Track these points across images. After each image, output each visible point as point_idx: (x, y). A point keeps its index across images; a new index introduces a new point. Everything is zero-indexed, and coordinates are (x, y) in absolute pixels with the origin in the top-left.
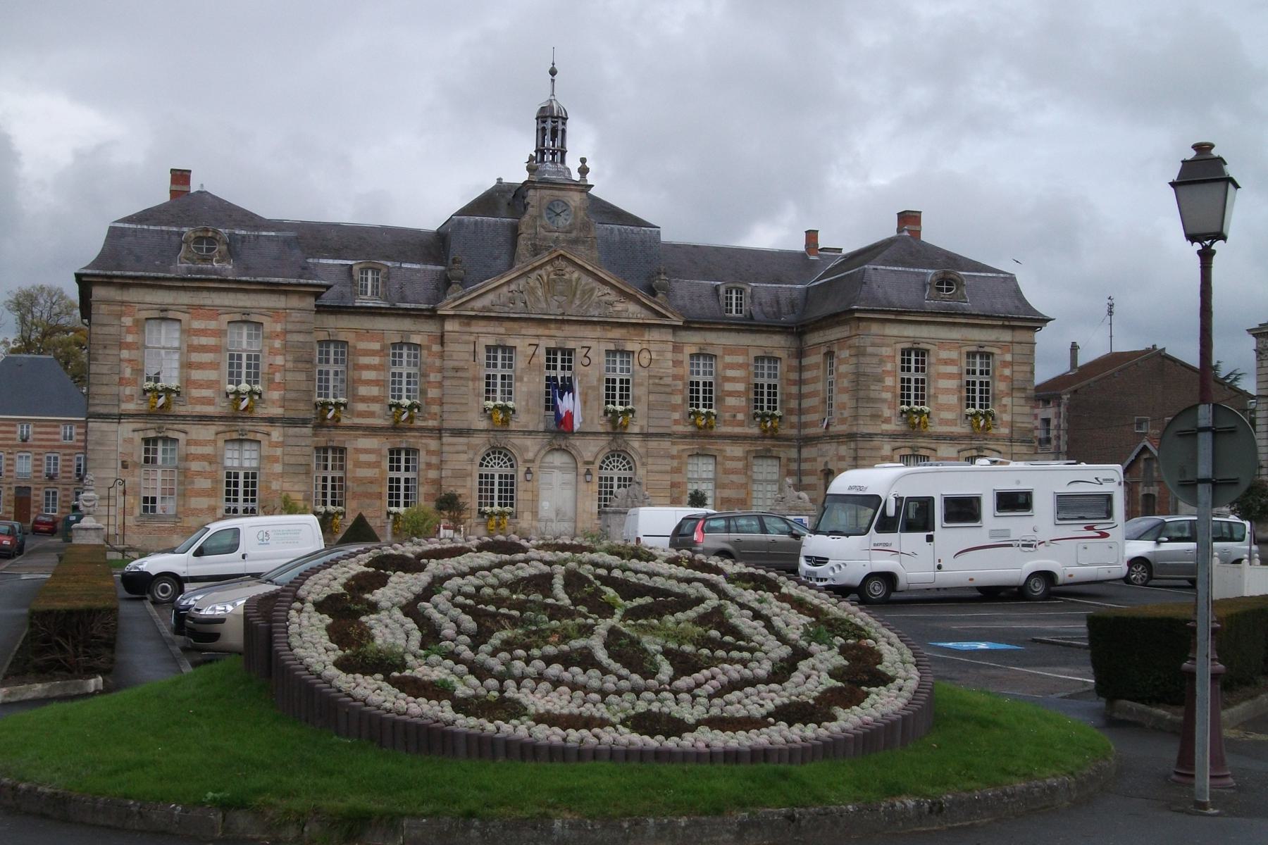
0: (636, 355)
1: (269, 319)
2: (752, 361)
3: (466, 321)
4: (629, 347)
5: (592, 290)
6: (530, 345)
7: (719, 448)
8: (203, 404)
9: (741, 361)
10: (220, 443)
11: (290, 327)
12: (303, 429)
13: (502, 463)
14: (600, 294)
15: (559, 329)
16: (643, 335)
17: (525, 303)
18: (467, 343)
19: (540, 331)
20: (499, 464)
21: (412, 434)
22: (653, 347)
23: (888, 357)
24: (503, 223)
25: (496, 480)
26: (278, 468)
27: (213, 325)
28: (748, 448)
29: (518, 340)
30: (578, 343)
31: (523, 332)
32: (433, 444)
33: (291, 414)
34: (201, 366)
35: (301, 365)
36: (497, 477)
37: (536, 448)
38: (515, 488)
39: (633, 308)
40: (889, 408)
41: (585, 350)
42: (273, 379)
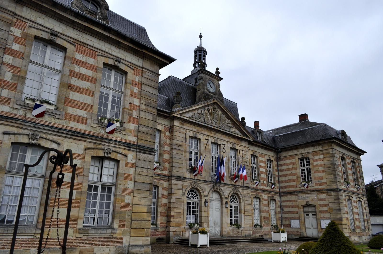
0: (239, 151)
1: (132, 71)
2: (266, 161)
3: (182, 122)
4: (237, 147)
5: (225, 120)
6: (206, 139)
7: (261, 195)
8: (77, 121)
9: (263, 160)
10: (88, 158)
11: (144, 81)
12: (149, 156)
14: (227, 123)
15: (215, 134)
16: (240, 143)
17: (204, 120)
18: (182, 133)
20: (193, 197)
21: (156, 177)
22: (244, 149)
26: (130, 185)
27: (91, 61)
28: (268, 196)
29: (201, 136)
30: (221, 142)
31: (203, 132)
33: (141, 143)
34: (79, 90)
35: (150, 109)
37: (209, 190)
39: (237, 131)
41: (224, 146)
42: (131, 114)
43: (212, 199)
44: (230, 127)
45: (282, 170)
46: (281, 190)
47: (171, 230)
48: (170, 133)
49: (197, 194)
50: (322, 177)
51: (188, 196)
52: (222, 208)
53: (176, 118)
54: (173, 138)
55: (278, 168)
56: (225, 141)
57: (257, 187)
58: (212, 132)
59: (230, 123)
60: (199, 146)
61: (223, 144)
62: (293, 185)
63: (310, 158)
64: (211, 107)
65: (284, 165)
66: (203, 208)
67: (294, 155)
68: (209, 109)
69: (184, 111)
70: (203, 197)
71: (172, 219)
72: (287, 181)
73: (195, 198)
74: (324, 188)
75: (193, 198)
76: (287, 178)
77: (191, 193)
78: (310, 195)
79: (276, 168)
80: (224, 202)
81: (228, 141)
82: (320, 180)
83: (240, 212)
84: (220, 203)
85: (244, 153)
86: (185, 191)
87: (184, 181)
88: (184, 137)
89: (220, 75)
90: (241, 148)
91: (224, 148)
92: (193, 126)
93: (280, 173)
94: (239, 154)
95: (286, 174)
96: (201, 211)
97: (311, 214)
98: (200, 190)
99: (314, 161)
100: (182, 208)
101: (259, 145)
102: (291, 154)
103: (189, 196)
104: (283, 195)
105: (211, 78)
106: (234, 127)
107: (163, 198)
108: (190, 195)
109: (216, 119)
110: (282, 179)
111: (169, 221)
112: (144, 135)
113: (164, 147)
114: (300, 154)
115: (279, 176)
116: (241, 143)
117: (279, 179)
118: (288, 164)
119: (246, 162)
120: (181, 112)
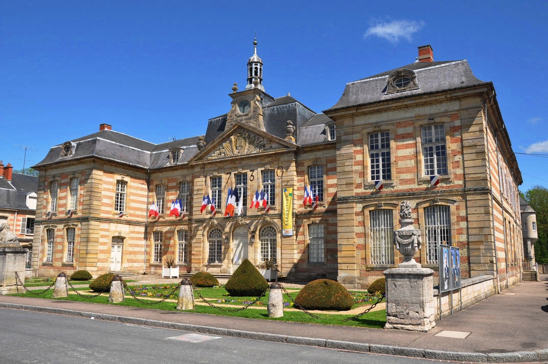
13: (218, 235)
14: (258, 142)
15: (240, 163)
16: (279, 160)
20: (217, 235)
23: (358, 140)
25: (216, 244)
35: (88, 193)
40: (360, 177)
71: (193, 257)
77: (215, 232)
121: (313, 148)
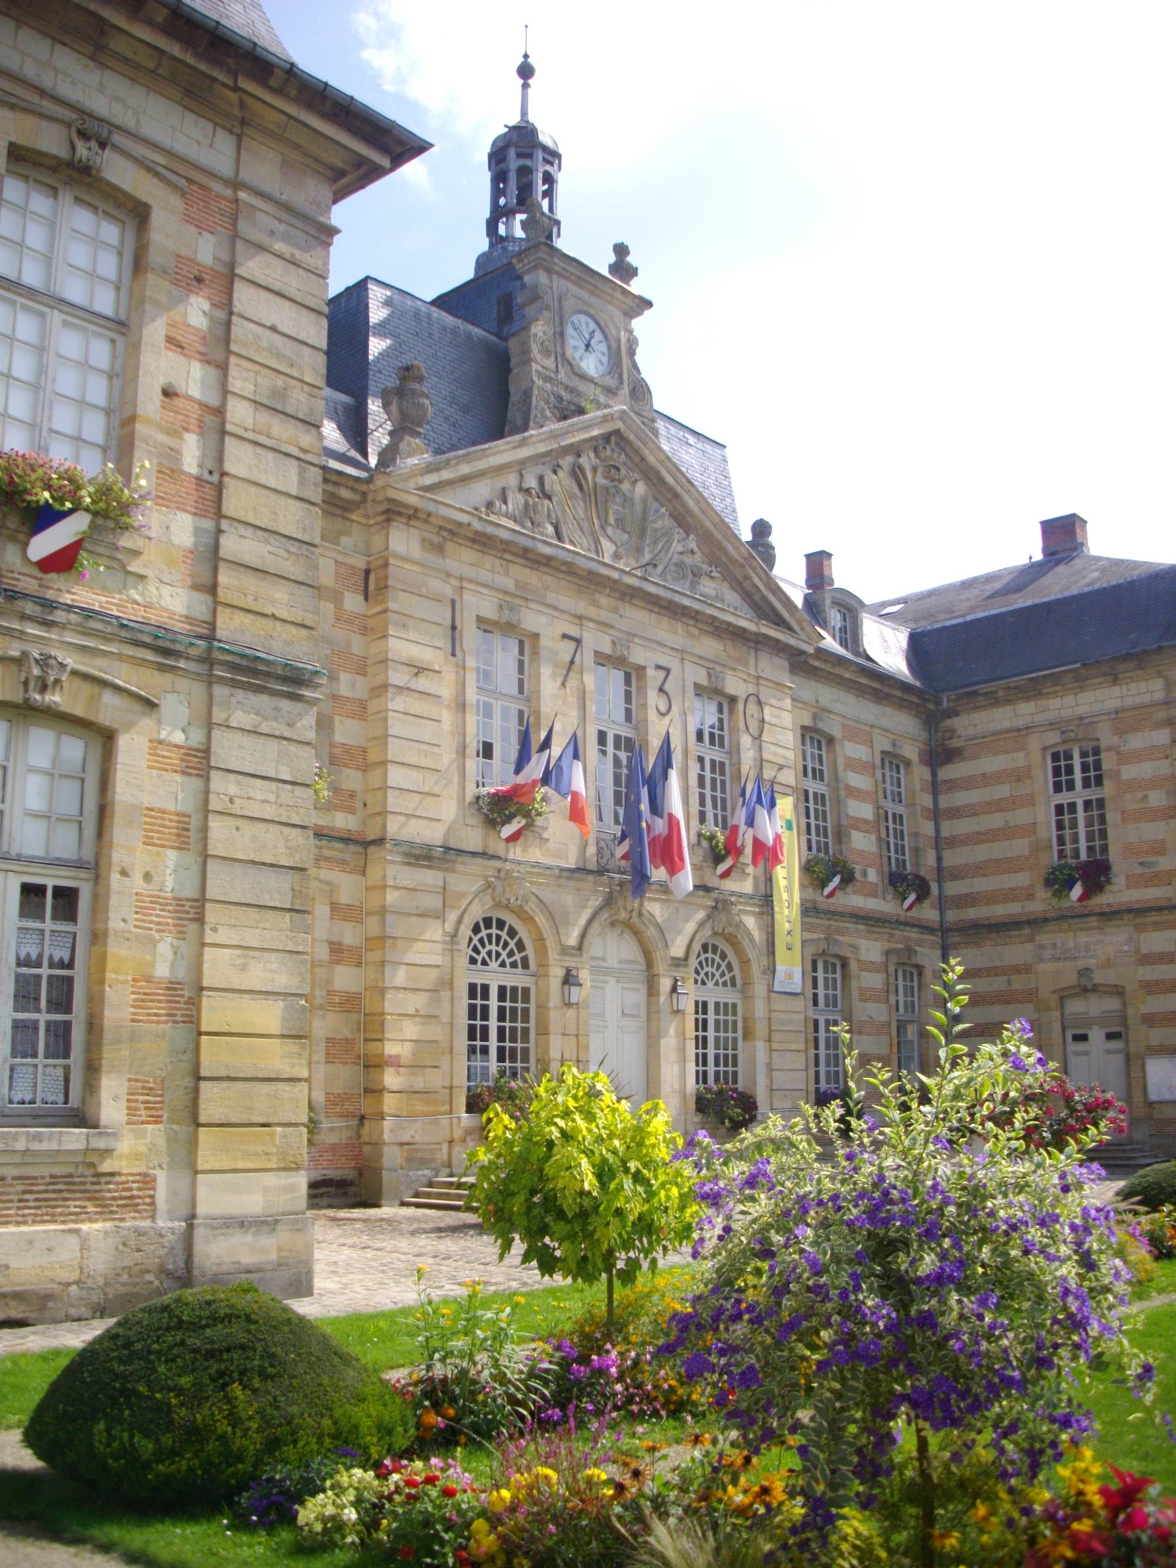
0: (740, 706)
1: (175, 201)
5: (668, 533)
6: (565, 636)
9: (864, 758)
13: (504, 954)
14: (680, 549)
15: (615, 610)
16: (746, 664)
19: (582, 606)
20: (498, 955)
24: (469, 336)
28: (887, 945)
29: (543, 620)
30: (649, 654)
31: (551, 597)
32: (348, 887)
36: (494, 993)
38: (532, 1024)
41: (662, 674)
43: (603, 964)
44: (696, 574)
45: (955, 813)
46: (952, 916)
47: (387, 1137)
48: (366, 599)
49: (520, 941)
50: (1163, 841)
51: (476, 950)
52: (652, 1011)
53: (399, 513)
54: (386, 629)
55: (935, 802)
56: (667, 651)
57: (832, 900)
58: (597, 596)
59: (692, 552)
60: (526, 672)
61: (658, 667)
62: (1013, 889)
63: (1103, 744)
64: (592, 455)
65: (969, 783)
66: (557, 1019)
67: (1019, 730)
68: (580, 468)
69: (446, 475)
70: (553, 954)
72: (981, 869)
73: (514, 965)
74: (1169, 899)
75: (503, 965)
76: (980, 853)
77: (489, 936)
78: (1101, 938)
79: (927, 800)
80: (665, 984)
81: (682, 652)
82: (1150, 859)
83: (748, 1035)
84: (643, 989)
85: (767, 717)
86: (459, 922)
87: (454, 871)
88: (448, 622)
89: (636, 287)
90: (751, 689)
91: (666, 688)
92: (497, 562)
93: (947, 829)
94: (742, 725)
95: (979, 833)
96: (544, 1032)
97: (1096, 1035)
98: (541, 920)
99: (1125, 758)
100: (445, 1018)
101: (841, 677)
102: (1006, 724)
103: (478, 953)
104: (958, 939)
105: (584, 295)
106: (714, 574)
107: (338, 962)
108: (484, 946)
109: (620, 524)
110: (952, 858)
111: (373, 1086)
112: (251, 583)
113: (337, 679)
114: (1052, 725)
115: (939, 843)
116: (752, 661)
117: (939, 859)
118: (986, 780)
119: (781, 767)
120: (429, 480)
121: (828, 667)
